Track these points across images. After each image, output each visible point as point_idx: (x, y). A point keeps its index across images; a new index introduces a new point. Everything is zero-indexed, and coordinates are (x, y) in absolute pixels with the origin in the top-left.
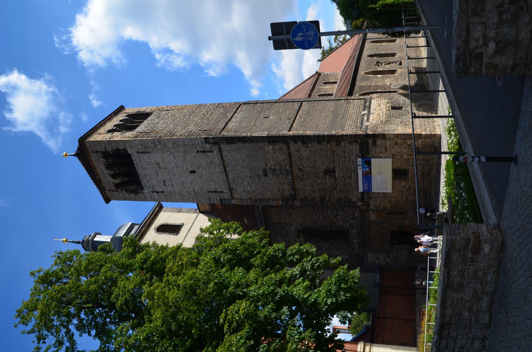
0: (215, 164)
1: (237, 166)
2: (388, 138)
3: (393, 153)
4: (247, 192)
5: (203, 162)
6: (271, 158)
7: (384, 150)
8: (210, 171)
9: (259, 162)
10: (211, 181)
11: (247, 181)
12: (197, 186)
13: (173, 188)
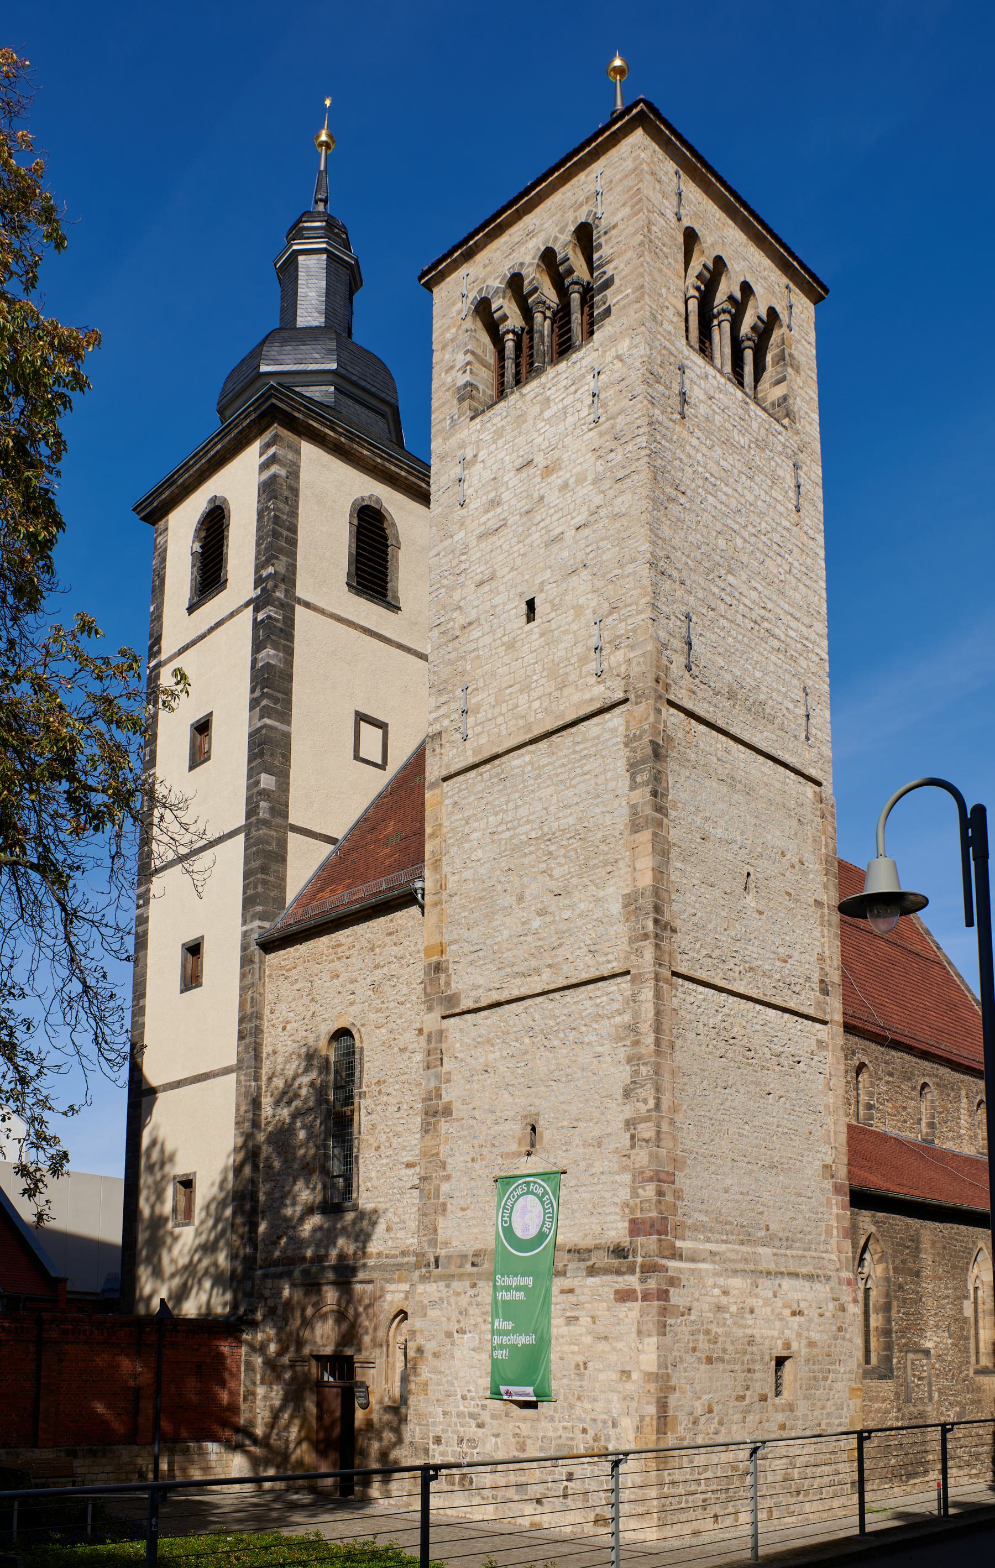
0: (556, 694)
1: (549, 782)
2: (640, 1347)
3: (590, 1365)
4: (467, 830)
5: (560, 646)
6: (577, 912)
7: (600, 1328)
8: (535, 678)
9: (566, 867)
10: (500, 690)
11: (500, 829)
12: (483, 635)
13: (475, 542)
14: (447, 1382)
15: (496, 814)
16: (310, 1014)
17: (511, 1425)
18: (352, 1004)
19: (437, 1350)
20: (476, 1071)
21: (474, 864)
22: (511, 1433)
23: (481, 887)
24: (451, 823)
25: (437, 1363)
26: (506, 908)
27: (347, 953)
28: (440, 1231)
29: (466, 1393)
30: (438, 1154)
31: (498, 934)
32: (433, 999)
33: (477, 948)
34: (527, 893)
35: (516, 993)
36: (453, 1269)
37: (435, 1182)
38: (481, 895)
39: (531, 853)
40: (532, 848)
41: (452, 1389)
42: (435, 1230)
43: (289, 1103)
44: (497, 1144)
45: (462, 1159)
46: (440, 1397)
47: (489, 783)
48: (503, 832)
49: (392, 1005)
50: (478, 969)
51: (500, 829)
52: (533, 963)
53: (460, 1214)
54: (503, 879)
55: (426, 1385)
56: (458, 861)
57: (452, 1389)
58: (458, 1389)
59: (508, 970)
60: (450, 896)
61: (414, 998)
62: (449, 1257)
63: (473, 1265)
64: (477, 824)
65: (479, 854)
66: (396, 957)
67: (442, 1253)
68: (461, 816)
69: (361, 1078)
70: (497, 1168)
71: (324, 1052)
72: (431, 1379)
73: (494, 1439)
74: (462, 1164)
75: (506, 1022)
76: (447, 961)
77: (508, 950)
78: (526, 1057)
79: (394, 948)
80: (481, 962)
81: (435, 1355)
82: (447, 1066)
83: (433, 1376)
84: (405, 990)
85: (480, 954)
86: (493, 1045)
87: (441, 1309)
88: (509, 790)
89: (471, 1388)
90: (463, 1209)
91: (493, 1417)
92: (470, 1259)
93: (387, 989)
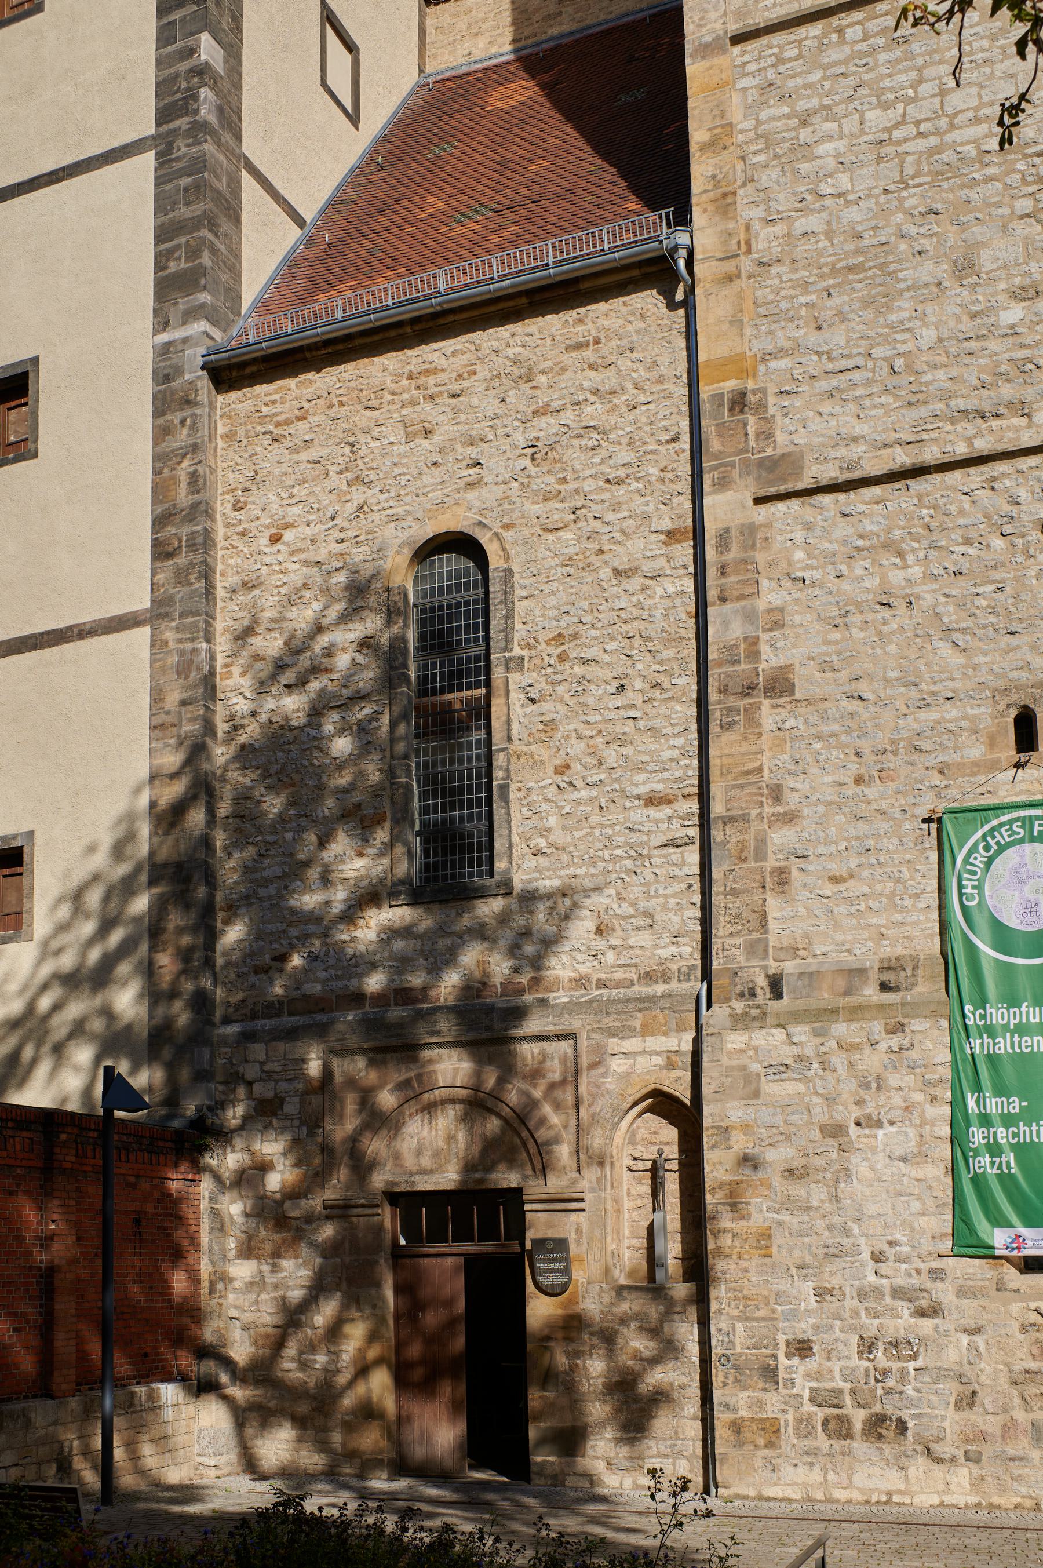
4: (805, 135)
11: (897, 134)
14: (830, 1228)
15: (885, 106)
16: (350, 508)
17: (1016, 1308)
18: (471, 485)
19: (795, 1164)
20: (858, 605)
21: (828, 202)
22: (1015, 1326)
23: (851, 246)
24: (759, 122)
25: (797, 1190)
26: (926, 285)
27: (456, 387)
28: (772, 925)
29: (885, 1247)
30: (760, 769)
31: (907, 336)
32: (732, 465)
33: (850, 363)
34: (985, 255)
35: (962, 450)
36: (825, 997)
37: (755, 827)
38: (851, 262)
39: (989, 179)
40: (992, 171)
41: (845, 1241)
42: (764, 924)
43: (301, 682)
44: (926, 746)
45: (828, 779)
46: (808, 1259)
47: (863, 46)
48: (906, 140)
49: (588, 485)
50: (852, 407)
51: (897, 134)
52: (1007, 391)
53: (828, 889)
54: (913, 230)
55: (765, 1236)
56: (781, 197)
57: (845, 1241)
58: (862, 1241)
59: (939, 406)
60: (762, 264)
61: (653, 471)
62: (810, 977)
63: (884, 987)
64: (831, 126)
65: (844, 181)
66: (596, 392)
67: (789, 967)
68: (786, 110)
69: (508, 632)
70: (929, 796)
71: (397, 581)
72: (781, 1223)
73: (965, 1339)
74: (830, 790)
75: (935, 507)
76: (763, 391)
77: (935, 367)
78: (997, 576)
79: (592, 374)
80: (860, 392)
81: (791, 1174)
82: (770, 595)
83: (786, 1217)
84: (625, 455)
85: (856, 376)
86: (901, 554)
87: (805, 1080)
88: (920, 61)
89: (898, 1236)
90: (834, 880)
91: (962, 1292)
92: (874, 977)
93: (574, 454)
